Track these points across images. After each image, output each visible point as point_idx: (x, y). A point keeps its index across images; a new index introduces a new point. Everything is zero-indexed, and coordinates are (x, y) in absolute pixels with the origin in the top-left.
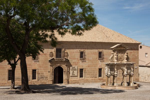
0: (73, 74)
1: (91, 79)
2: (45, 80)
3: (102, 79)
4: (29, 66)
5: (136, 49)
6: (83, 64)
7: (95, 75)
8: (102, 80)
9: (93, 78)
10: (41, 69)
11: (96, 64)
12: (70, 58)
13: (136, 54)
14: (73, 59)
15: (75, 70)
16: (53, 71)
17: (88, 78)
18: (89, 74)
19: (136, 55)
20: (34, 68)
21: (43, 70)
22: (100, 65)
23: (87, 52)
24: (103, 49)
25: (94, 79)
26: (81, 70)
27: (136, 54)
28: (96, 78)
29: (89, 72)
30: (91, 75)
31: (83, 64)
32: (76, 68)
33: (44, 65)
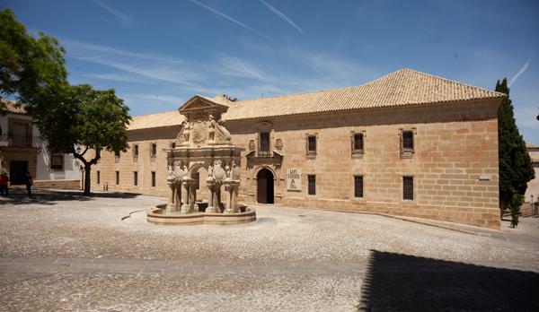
0: (292, 186)
1: (333, 200)
3: (362, 204)
5: (468, 116)
6: (315, 165)
7: (343, 192)
11: (346, 165)
13: (485, 132)
15: (297, 176)
17: (327, 196)
18: (330, 189)
19: (485, 135)
22: (358, 167)
23: (323, 135)
24: (365, 125)
26: (312, 179)
27: (485, 132)
28: (347, 198)
29: (329, 184)
31: (315, 165)
32: (299, 172)
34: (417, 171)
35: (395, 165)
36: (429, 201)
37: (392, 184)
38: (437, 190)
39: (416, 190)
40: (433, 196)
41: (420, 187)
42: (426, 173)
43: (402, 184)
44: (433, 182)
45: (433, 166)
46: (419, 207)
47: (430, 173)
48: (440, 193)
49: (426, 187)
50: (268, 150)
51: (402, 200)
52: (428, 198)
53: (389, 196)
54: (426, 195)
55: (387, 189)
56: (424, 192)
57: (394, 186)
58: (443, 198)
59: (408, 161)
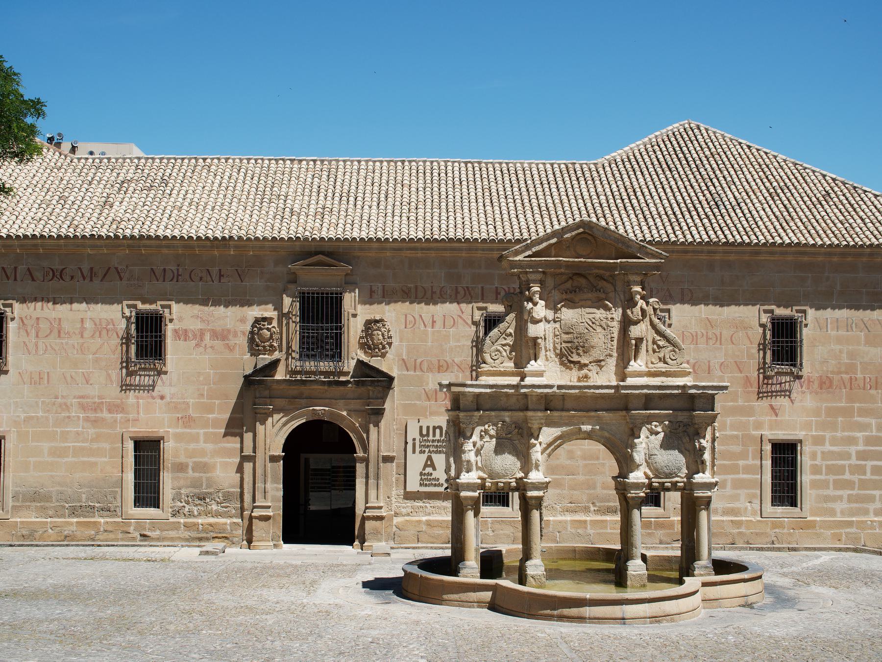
1: (568, 517)
2: (218, 514)
4: (110, 411)
8: (660, 533)
9: (586, 510)
10: (195, 439)
12: (405, 364)
14: (430, 370)
16: (279, 452)
20: (144, 430)
21: (210, 446)
25: (594, 522)
30: (572, 488)
33: (212, 412)
34: (807, 426)
35: (750, 412)
36: (838, 506)
37: (741, 463)
38: (855, 478)
39: (806, 478)
40: (845, 493)
41: (816, 470)
42: (828, 435)
43: (768, 463)
44: (847, 456)
45: (847, 412)
46: (811, 525)
47: (839, 434)
48: (864, 484)
49: (831, 470)
50: (335, 350)
51: (768, 508)
52: (834, 499)
53: (735, 498)
54: (831, 492)
55: (729, 477)
56: (824, 484)
57: (748, 469)
58: (872, 499)
59: (781, 402)
